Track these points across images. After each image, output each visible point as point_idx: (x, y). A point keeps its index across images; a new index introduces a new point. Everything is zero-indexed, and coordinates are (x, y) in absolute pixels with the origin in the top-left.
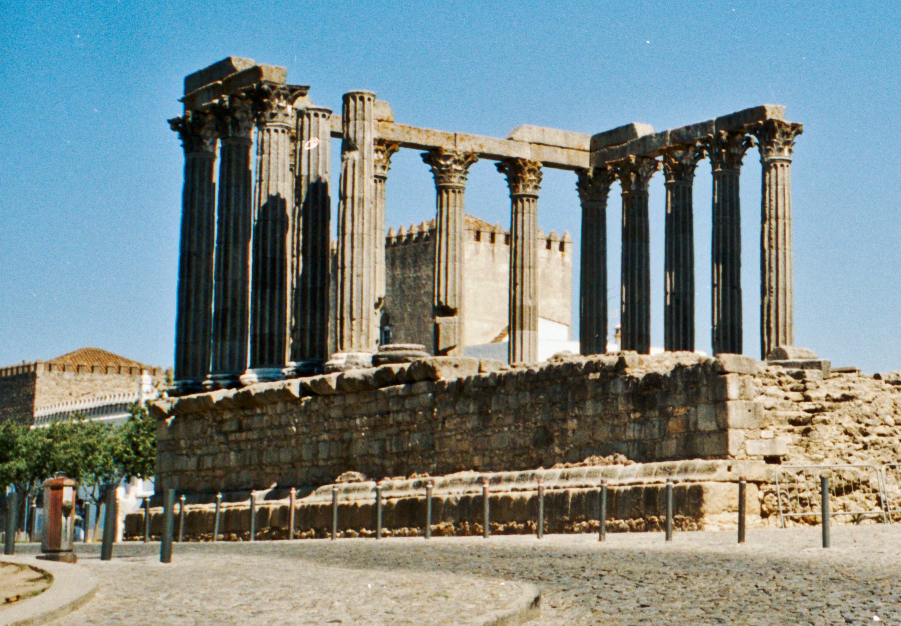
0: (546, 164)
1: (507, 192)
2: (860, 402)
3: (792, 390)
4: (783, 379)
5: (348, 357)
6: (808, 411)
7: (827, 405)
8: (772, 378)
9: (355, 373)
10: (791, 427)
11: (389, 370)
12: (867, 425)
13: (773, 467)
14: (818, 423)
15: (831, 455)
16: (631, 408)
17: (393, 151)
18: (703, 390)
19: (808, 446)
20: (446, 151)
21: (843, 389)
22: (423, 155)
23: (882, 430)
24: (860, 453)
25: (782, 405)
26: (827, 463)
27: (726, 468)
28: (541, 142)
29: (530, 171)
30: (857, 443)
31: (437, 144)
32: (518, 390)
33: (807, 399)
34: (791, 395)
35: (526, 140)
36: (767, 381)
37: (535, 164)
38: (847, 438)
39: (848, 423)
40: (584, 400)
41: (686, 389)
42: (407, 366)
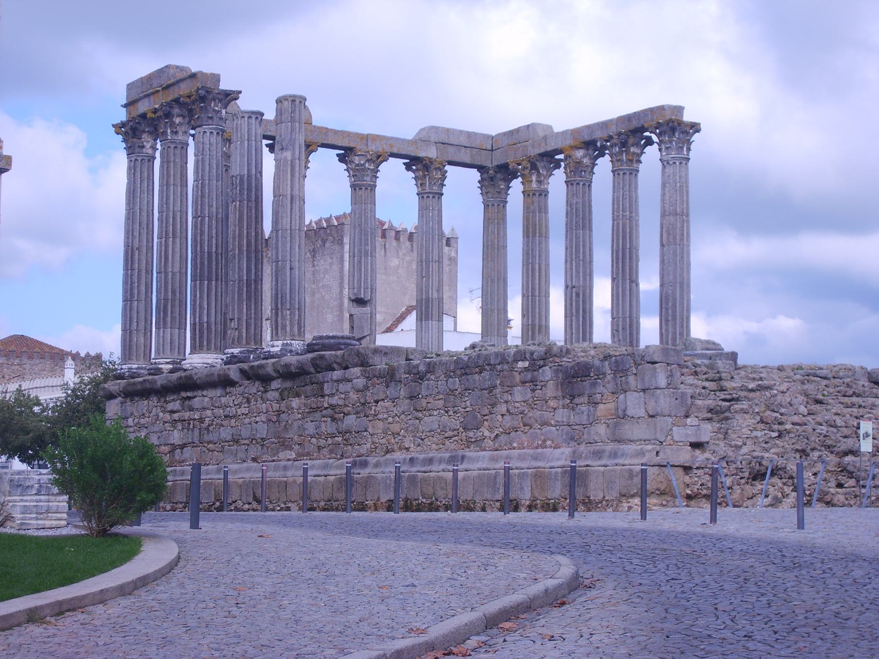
0: (451, 163)
1: (415, 190)
5: (283, 344)
6: (724, 400)
7: (743, 394)
9: (290, 359)
10: (709, 415)
11: (322, 357)
12: (781, 414)
13: (698, 452)
14: (736, 412)
16: (560, 394)
17: (312, 151)
18: (631, 379)
19: (726, 433)
20: (360, 150)
21: (754, 379)
22: (338, 155)
23: (796, 419)
26: (745, 450)
28: (447, 141)
31: (352, 145)
33: (722, 390)
34: (707, 384)
35: (432, 140)
38: (762, 426)
42: (339, 353)
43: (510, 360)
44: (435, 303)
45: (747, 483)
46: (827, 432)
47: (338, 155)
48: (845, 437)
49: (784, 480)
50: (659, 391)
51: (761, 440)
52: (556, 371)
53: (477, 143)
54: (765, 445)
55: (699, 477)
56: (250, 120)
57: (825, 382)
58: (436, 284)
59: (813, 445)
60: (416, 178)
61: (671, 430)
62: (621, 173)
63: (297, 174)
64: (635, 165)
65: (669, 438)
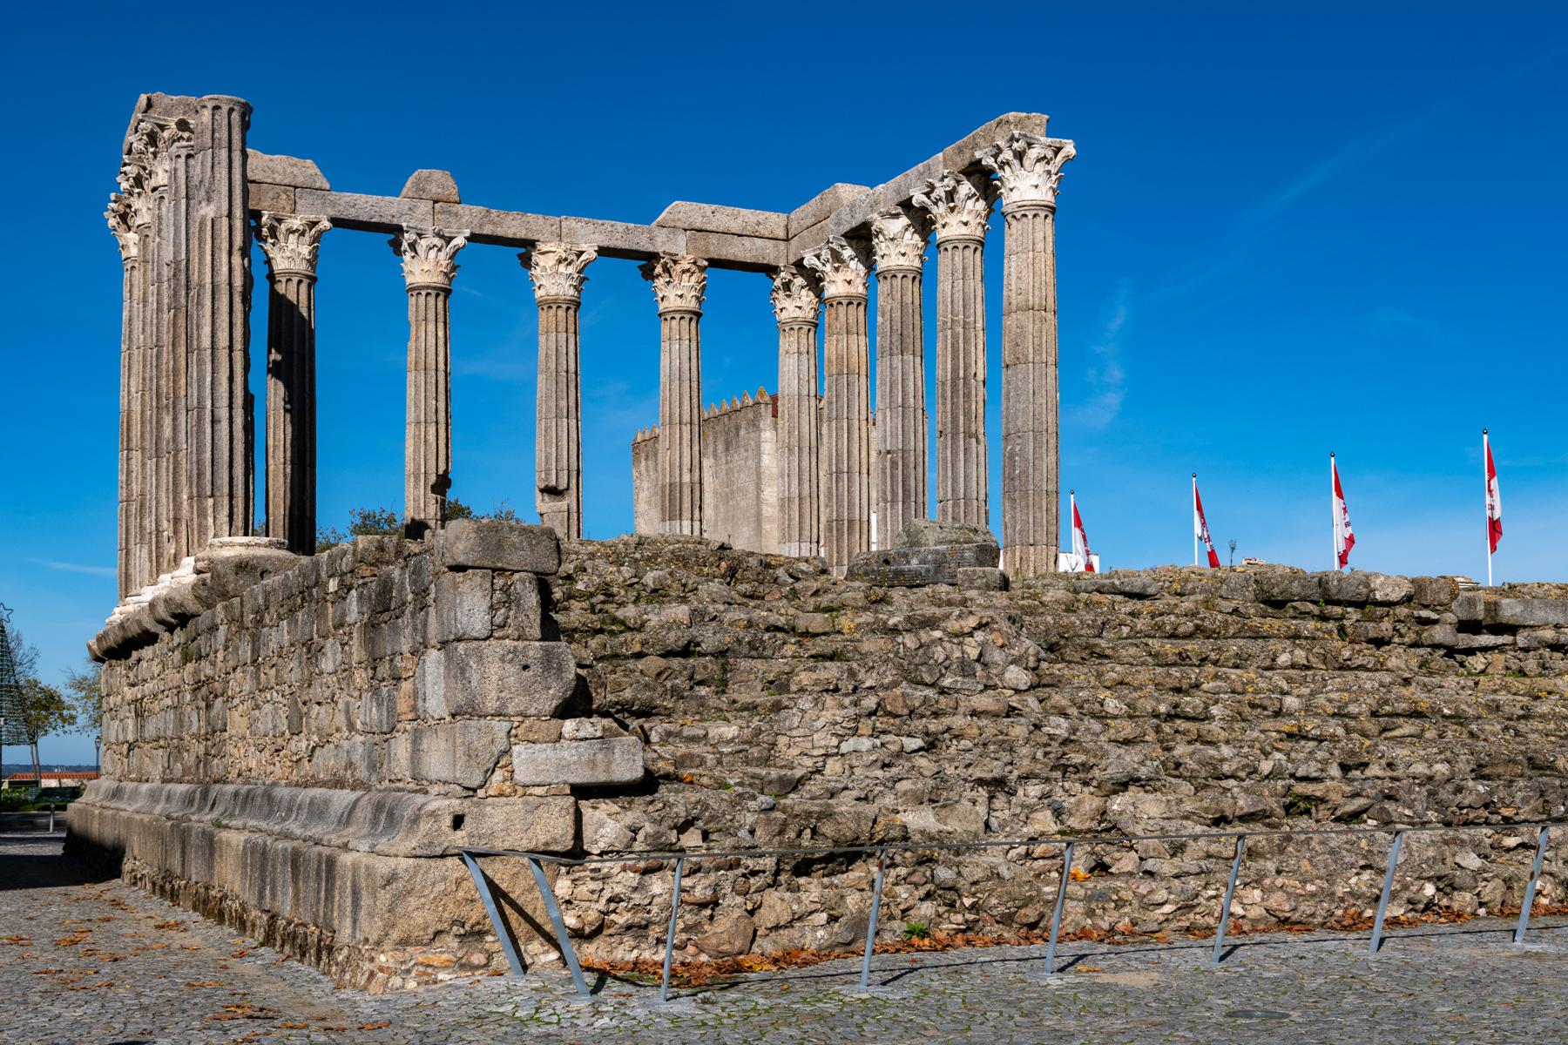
2: (938, 634)
3: (817, 609)
4: (798, 586)
12: (943, 692)
14: (802, 690)
15: (833, 766)
16: (363, 655)
22: (520, 256)
23: (984, 701)
27: (448, 820)
29: (683, 272)
32: (280, 618)
40: (325, 637)
41: (413, 614)
43: (323, 575)
44: (686, 491)
45: (774, 884)
46: (1074, 730)
47: (520, 256)
48: (1127, 742)
49: (903, 871)
50: (461, 646)
52: (360, 597)
54: (880, 773)
55: (605, 878)
56: (192, 162)
57: (1132, 605)
61: (507, 752)
62: (950, 247)
65: (498, 776)
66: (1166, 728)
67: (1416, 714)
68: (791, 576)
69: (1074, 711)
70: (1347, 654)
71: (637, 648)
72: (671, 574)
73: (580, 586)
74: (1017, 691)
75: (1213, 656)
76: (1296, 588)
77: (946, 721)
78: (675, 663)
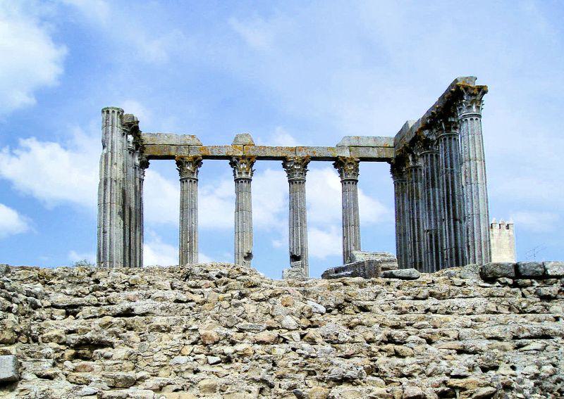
1: (340, 179)
2: (245, 300)
8: (209, 278)
12: (241, 331)
23: (264, 336)
24: (216, 369)
25: (167, 309)
28: (358, 145)
29: (349, 164)
30: (212, 355)
31: (284, 155)
35: (346, 145)
36: (202, 283)
37: (352, 159)
38: (197, 348)
39: (208, 328)
48: (348, 357)
51: (183, 368)
53: (382, 144)
54: (191, 376)
58: (353, 241)
59: (281, 372)
60: (340, 172)
63: (109, 163)
64: (453, 131)
66: (374, 348)
67: (545, 336)
68: (217, 276)
69: (319, 340)
70: (524, 304)
71: (103, 312)
72: (142, 277)
73: (101, 285)
74: (289, 330)
75: (433, 308)
76: (498, 270)
77: (239, 347)
78: (116, 320)
